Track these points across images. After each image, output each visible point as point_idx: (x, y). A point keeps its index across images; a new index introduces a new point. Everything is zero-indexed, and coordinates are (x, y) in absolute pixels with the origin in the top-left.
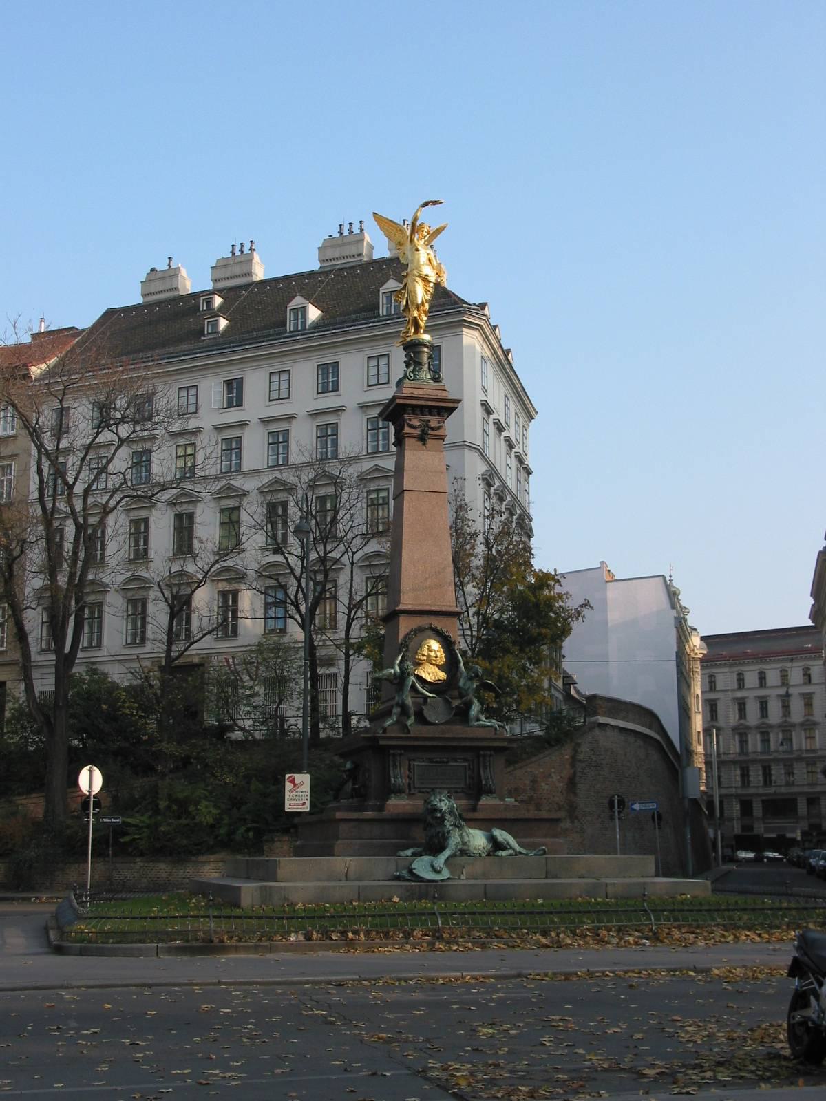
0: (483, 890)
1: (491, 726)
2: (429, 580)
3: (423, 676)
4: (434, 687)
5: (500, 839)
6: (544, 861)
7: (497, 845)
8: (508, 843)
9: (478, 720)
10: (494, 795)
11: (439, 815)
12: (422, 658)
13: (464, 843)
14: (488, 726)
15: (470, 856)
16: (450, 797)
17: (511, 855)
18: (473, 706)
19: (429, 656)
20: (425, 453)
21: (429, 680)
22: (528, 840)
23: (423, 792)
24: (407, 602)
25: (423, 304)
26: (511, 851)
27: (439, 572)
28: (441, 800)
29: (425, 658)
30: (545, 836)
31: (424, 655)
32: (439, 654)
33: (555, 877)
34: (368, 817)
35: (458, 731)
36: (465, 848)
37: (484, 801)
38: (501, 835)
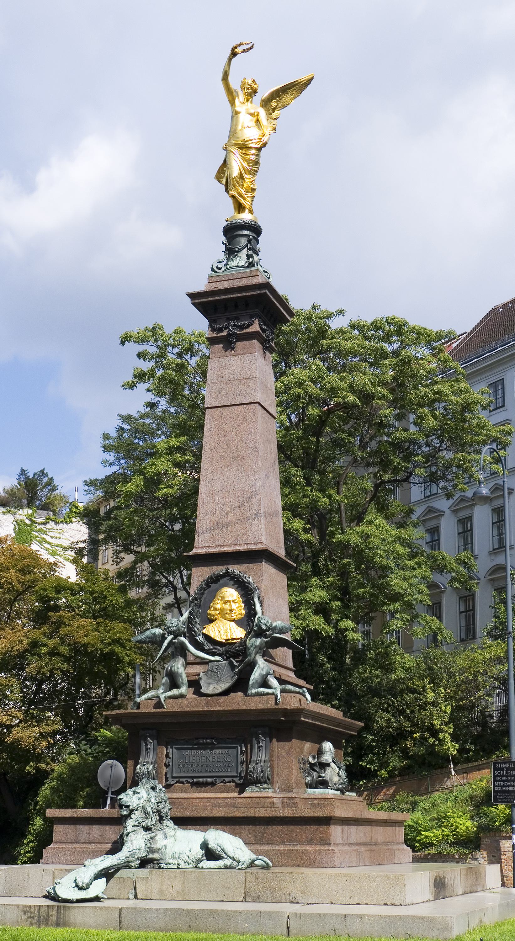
0: (117, 915)
1: (273, 694)
2: (230, 514)
5: (212, 845)
6: (242, 877)
7: (210, 854)
8: (223, 850)
9: (265, 684)
10: (265, 785)
11: (125, 813)
12: (213, 612)
13: (152, 851)
14: (268, 694)
15: (160, 868)
16: (153, 789)
17: (226, 867)
20: (234, 358)
22: (281, 848)
23: (182, 783)
24: (203, 544)
25: (241, 177)
26: (228, 862)
27: (243, 503)
28: (135, 793)
29: (218, 612)
30: (310, 842)
31: (215, 609)
32: (234, 606)
33: (257, 899)
34: (84, 815)
35: (238, 702)
36: (156, 856)
37: (249, 792)
38: (219, 838)
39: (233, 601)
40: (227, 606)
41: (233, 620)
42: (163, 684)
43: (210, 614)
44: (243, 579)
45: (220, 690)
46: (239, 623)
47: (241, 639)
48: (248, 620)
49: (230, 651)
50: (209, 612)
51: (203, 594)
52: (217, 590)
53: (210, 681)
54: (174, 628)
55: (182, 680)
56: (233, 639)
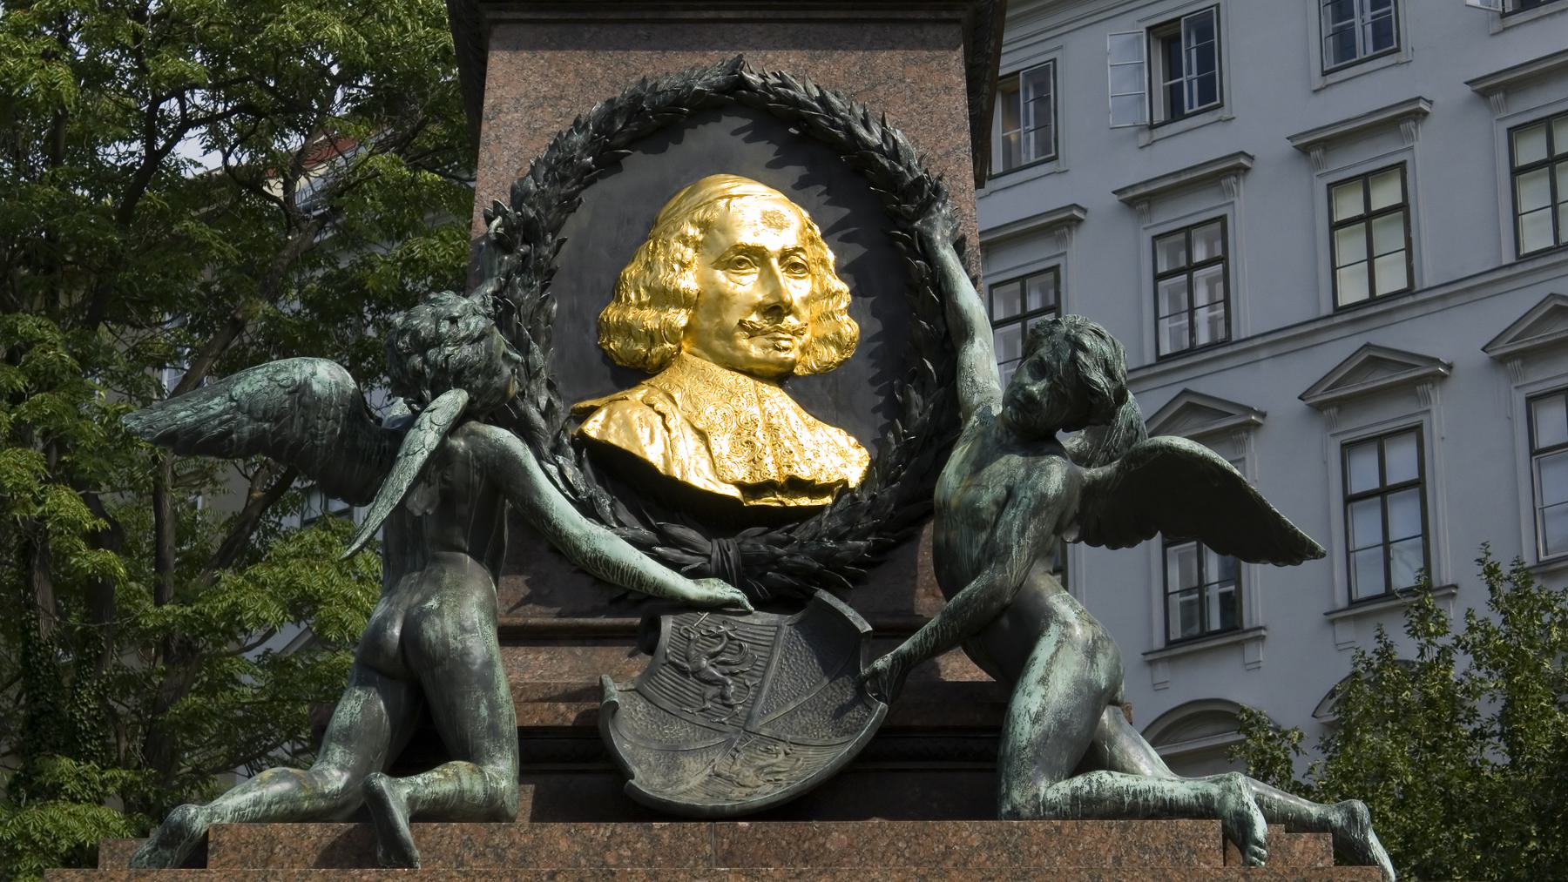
1: (1203, 810)
3: (653, 454)
4: (749, 531)
12: (650, 318)
14: (1169, 810)
18: (1044, 649)
19: (712, 303)
21: (700, 477)
29: (680, 318)
31: (666, 297)
32: (796, 289)
39: (784, 256)
40: (746, 286)
41: (782, 377)
42: (346, 737)
43: (627, 330)
44: (849, 130)
45: (765, 792)
46: (820, 394)
47: (840, 489)
48: (901, 370)
49: (775, 559)
50: (612, 314)
51: (569, 204)
52: (664, 192)
53: (678, 731)
54: (467, 350)
55: (493, 707)
56: (796, 485)
